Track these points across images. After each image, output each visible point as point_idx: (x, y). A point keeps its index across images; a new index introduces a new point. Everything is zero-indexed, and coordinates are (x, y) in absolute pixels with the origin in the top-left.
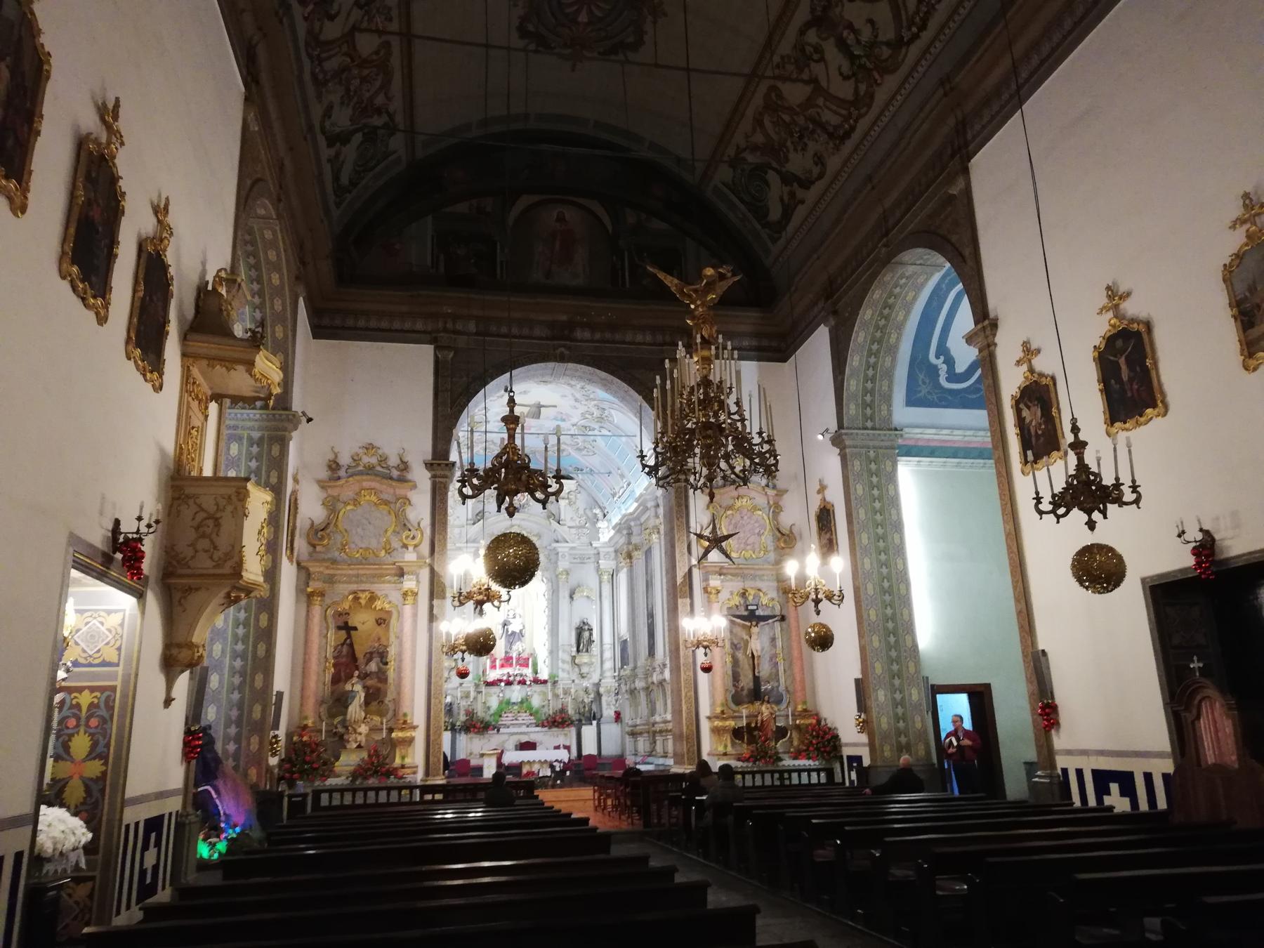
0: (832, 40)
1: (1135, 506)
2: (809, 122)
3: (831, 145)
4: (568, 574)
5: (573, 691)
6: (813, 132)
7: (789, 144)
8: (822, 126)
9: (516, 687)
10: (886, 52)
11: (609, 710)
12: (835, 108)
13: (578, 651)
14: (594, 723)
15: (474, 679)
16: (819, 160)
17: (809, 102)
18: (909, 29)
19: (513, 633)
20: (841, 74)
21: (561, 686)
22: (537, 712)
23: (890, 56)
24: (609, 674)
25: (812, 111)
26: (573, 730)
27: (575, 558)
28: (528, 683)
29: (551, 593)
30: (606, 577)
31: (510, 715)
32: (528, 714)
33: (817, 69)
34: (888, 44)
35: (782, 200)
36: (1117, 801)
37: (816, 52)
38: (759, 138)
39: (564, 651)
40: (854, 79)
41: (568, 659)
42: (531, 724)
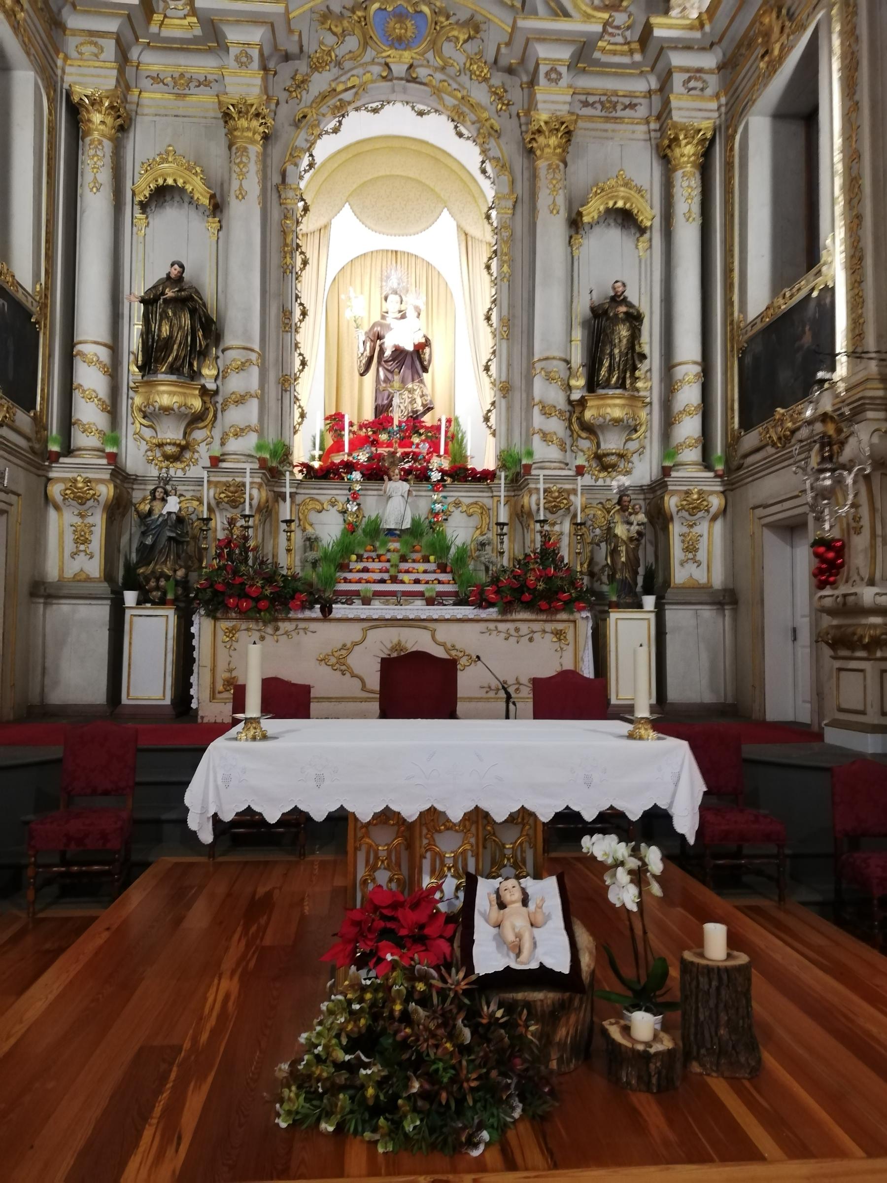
4: (568, 133)
5: (578, 501)
9: (397, 487)
11: (691, 568)
13: (592, 385)
14: (649, 601)
15: (259, 448)
19: (399, 354)
21: (541, 486)
22: (462, 557)
24: (692, 455)
26: (584, 622)
27: (586, 104)
28: (435, 476)
29: (510, 204)
30: (688, 151)
31: (377, 565)
32: (432, 566)
39: (549, 378)
41: (556, 397)
42: (440, 594)
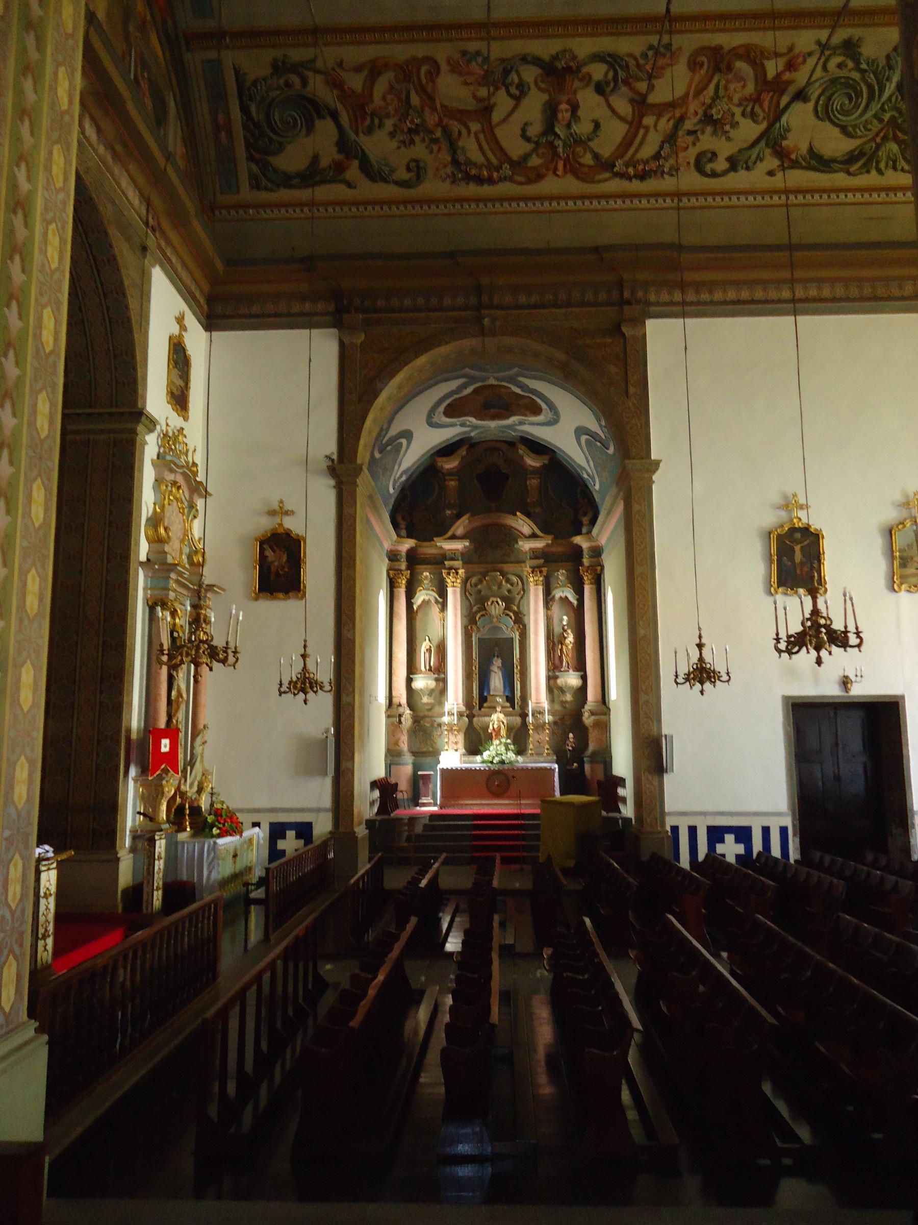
0: (545, 97)
1: (857, 649)
2: (440, 129)
3: (449, 170)
6: (436, 141)
7: (389, 124)
8: (453, 148)
10: (588, 159)
12: (486, 147)
16: (417, 170)
17: (462, 115)
18: (627, 165)
20: (524, 130)
23: (590, 167)
25: (455, 126)
33: (502, 101)
34: (596, 156)
35: (315, 159)
36: (730, 849)
37: (517, 88)
38: (356, 82)
40: (532, 146)
